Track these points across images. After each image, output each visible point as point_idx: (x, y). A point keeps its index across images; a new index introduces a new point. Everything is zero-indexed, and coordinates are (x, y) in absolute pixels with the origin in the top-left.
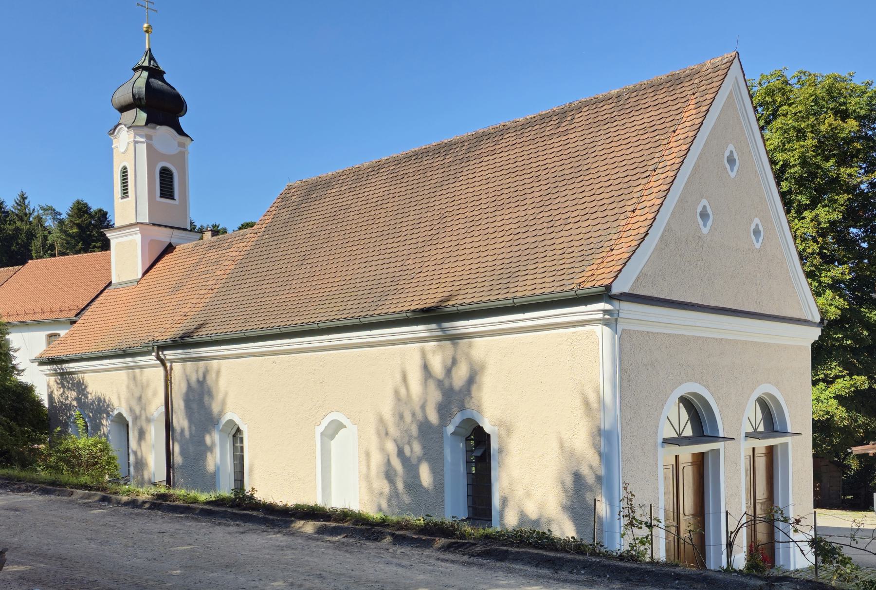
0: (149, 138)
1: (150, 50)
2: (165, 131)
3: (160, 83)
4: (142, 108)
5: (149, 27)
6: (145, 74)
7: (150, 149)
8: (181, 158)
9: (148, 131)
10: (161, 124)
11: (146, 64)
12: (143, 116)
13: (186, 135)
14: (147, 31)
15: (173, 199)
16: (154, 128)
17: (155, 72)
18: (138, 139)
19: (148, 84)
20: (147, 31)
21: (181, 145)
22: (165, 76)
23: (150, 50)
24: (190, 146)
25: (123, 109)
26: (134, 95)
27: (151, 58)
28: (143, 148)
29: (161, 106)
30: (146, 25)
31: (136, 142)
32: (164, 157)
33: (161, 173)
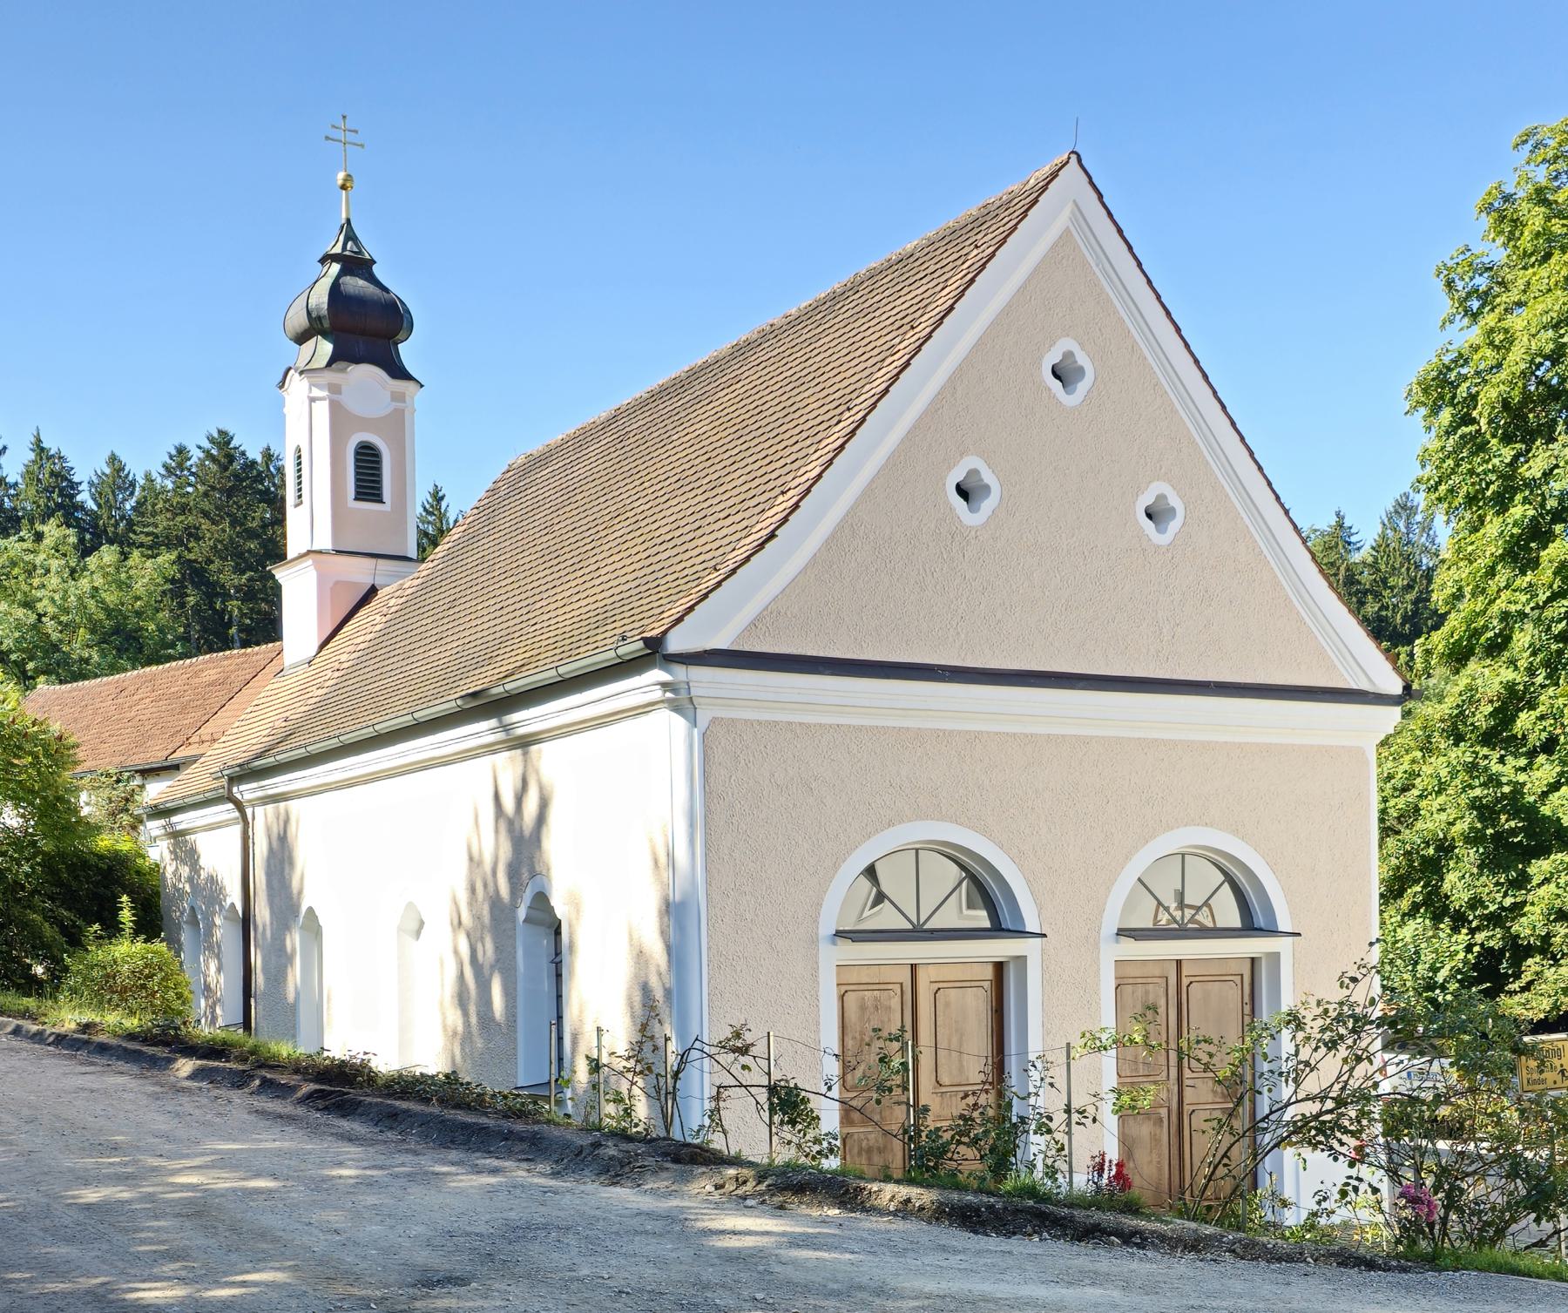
0: (334, 389)
1: (348, 221)
2: (366, 374)
3: (361, 282)
4: (325, 335)
5: (348, 178)
6: (335, 268)
7: (336, 411)
8: (397, 423)
9: (331, 376)
10: (357, 361)
11: (338, 250)
12: (326, 348)
13: (407, 376)
14: (343, 187)
15: (381, 502)
16: (344, 370)
17: (357, 264)
18: (316, 392)
19: (335, 290)
20: (343, 187)
21: (399, 397)
22: (375, 268)
23: (348, 221)
24: (419, 399)
25: (301, 339)
26: (309, 313)
27: (351, 236)
28: (322, 410)
29: (363, 327)
30: (341, 176)
31: (312, 400)
32: (366, 424)
33: (357, 453)
